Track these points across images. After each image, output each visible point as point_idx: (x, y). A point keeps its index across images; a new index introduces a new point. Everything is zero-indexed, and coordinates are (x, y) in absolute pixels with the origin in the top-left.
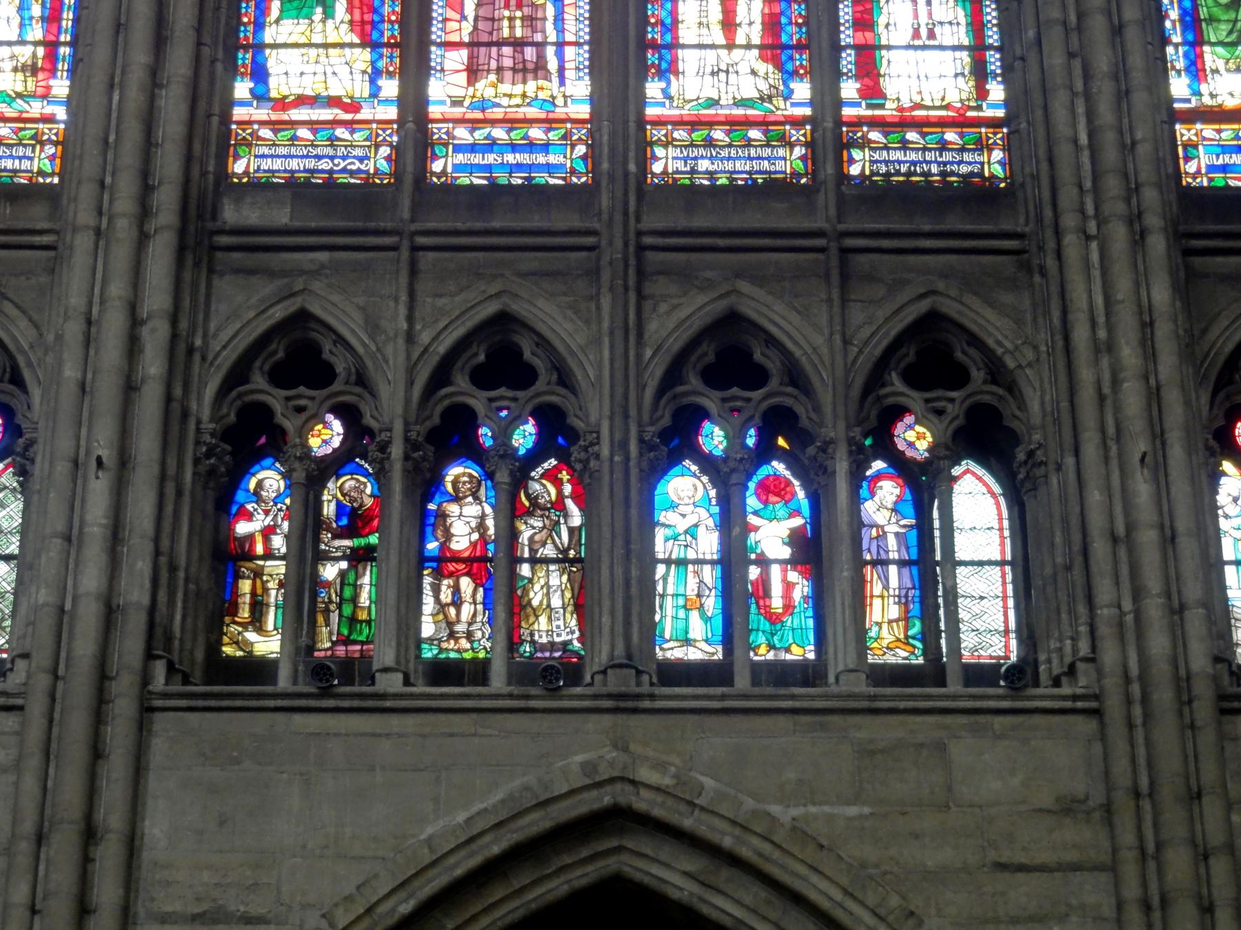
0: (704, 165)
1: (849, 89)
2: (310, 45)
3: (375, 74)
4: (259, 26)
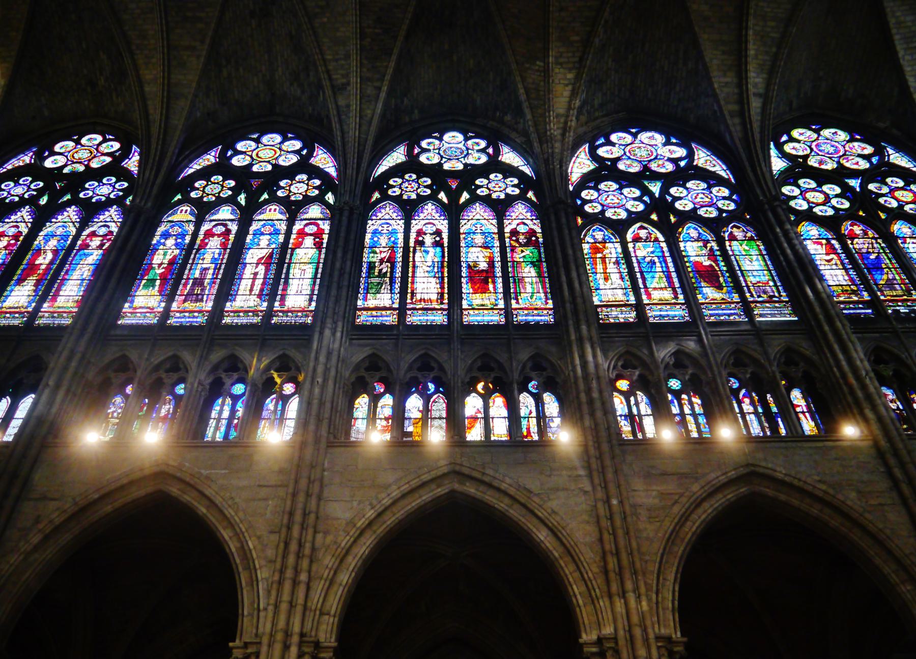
4: (136, 291)
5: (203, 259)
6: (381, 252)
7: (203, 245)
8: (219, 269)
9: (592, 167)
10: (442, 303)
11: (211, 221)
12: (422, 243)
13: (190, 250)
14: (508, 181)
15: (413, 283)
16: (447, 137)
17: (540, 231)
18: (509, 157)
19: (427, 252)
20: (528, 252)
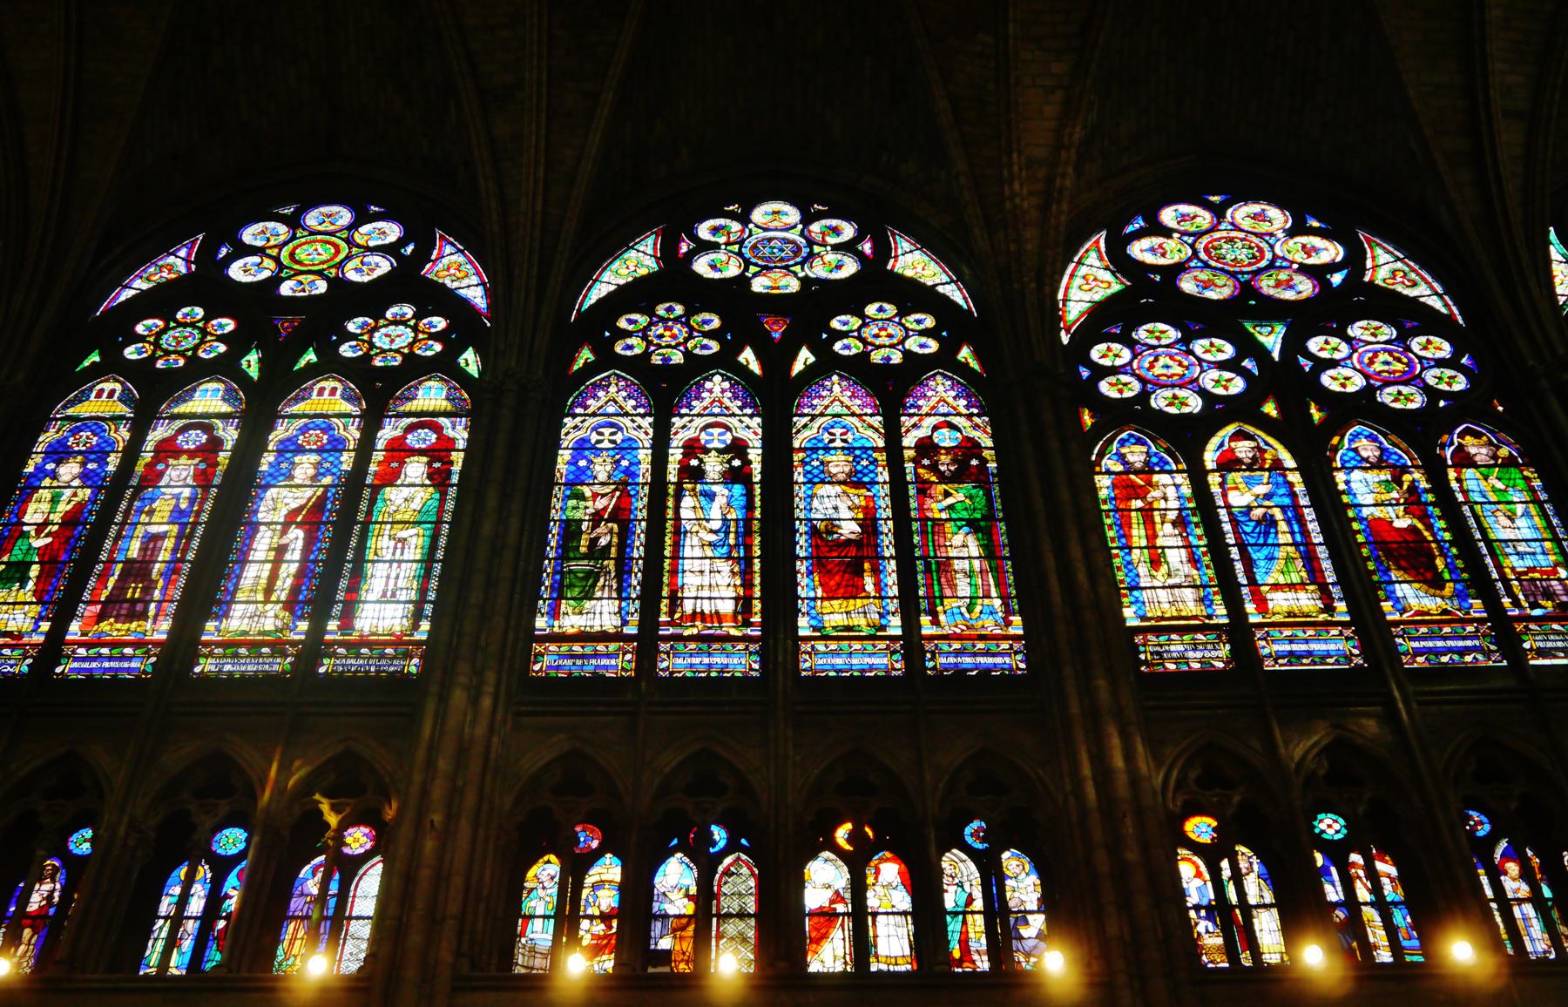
0: (228, 668)
5: (151, 513)
6: (595, 496)
7: (152, 477)
8: (190, 537)
9: (1117, 287)
10: (747, 624)
11: (174, 417)
12: (697, 475)
13: (118, 491)
14: (910, 321)
15: (674, 572)
16: (759, 214)
17: (990, 443)
18: (913, 262)
19: (711, 496)
20: (960, 497)
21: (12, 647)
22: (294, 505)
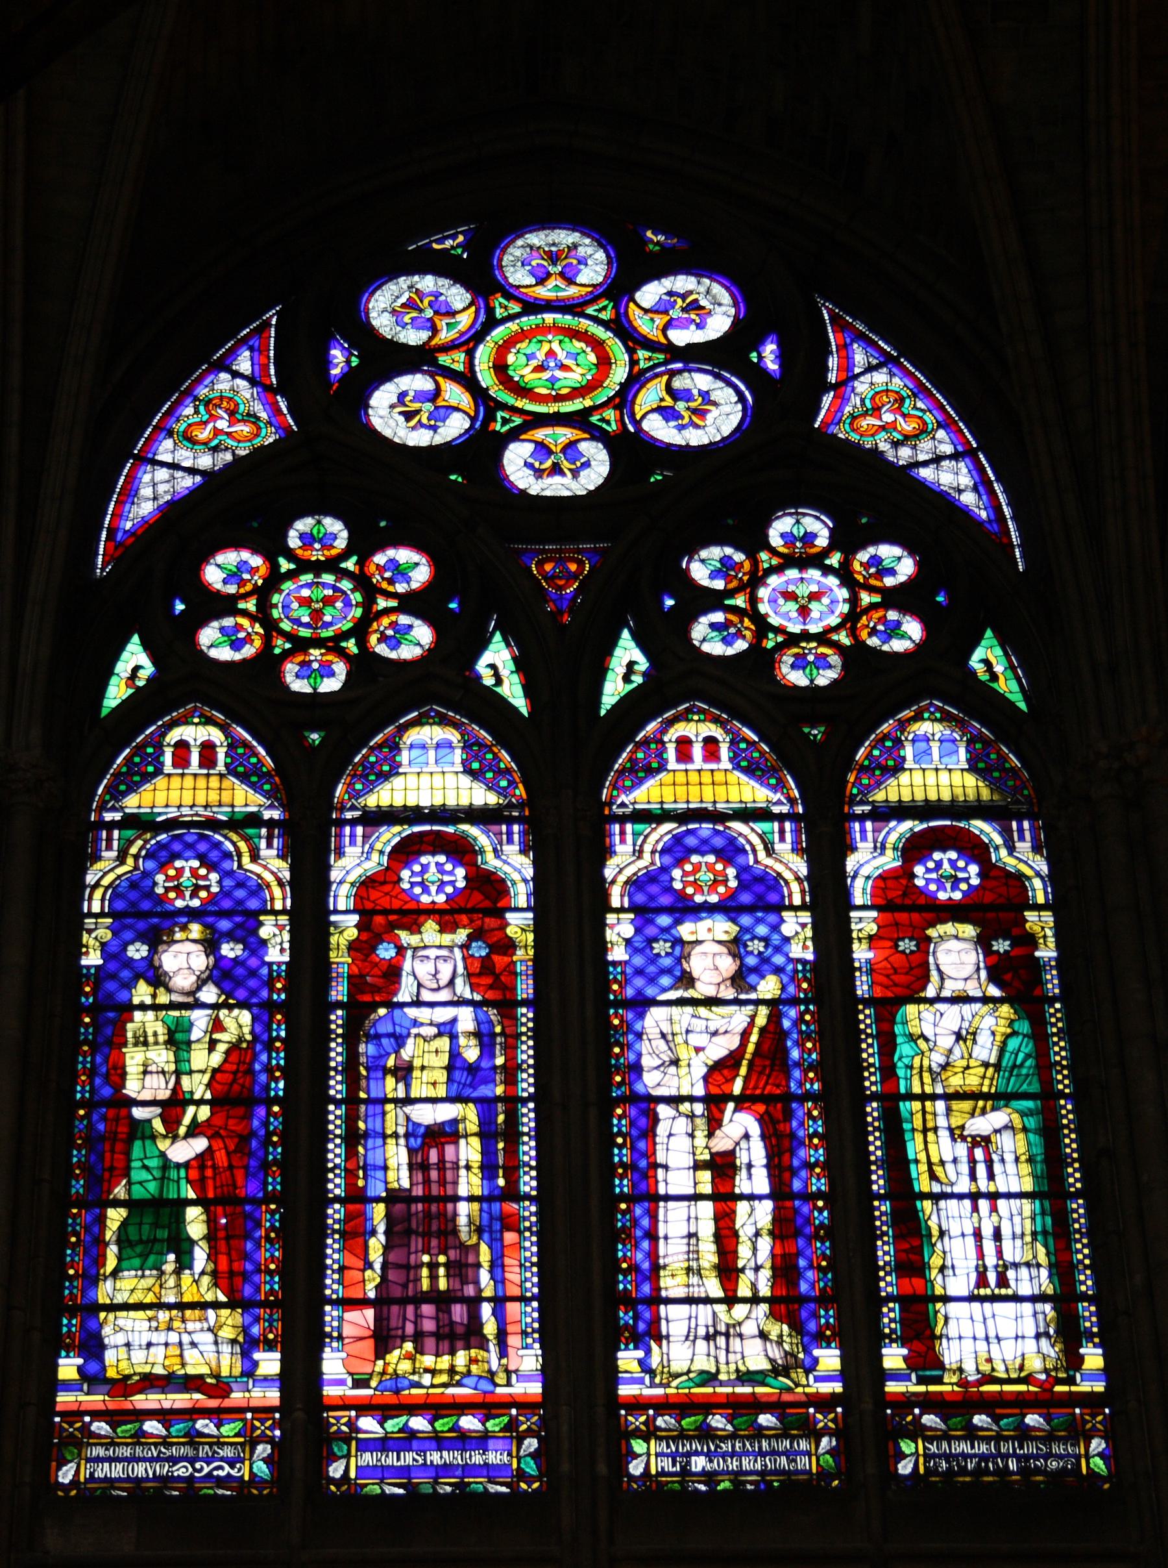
0: (699, 1463)
1: (893, 1357)
2: (160, 1306)
3: (248, 1346)
4: (92, 1279)
5: (404, 1072)
7: (378, 984)
8: (512, 1135)
13: (316, 1023)
21: (219, 1415)
22: (718, 1050)
